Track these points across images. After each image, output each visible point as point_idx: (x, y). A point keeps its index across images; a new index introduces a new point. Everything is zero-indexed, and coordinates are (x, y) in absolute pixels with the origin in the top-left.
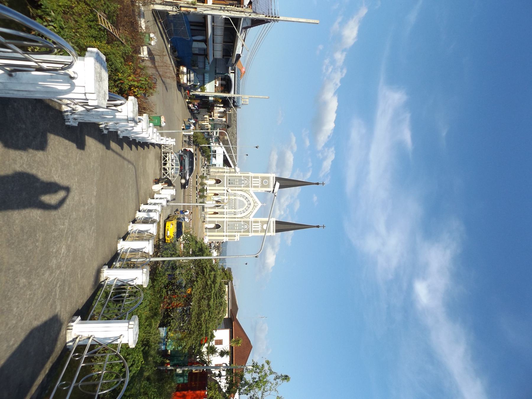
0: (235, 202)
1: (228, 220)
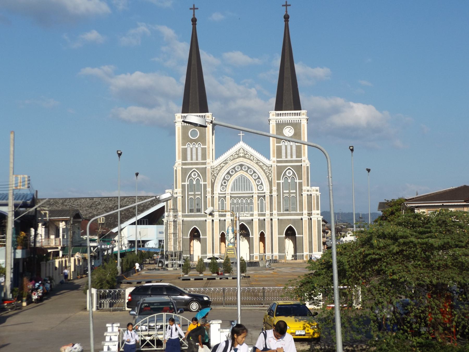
0: (237, 197)
1: (275, 212)
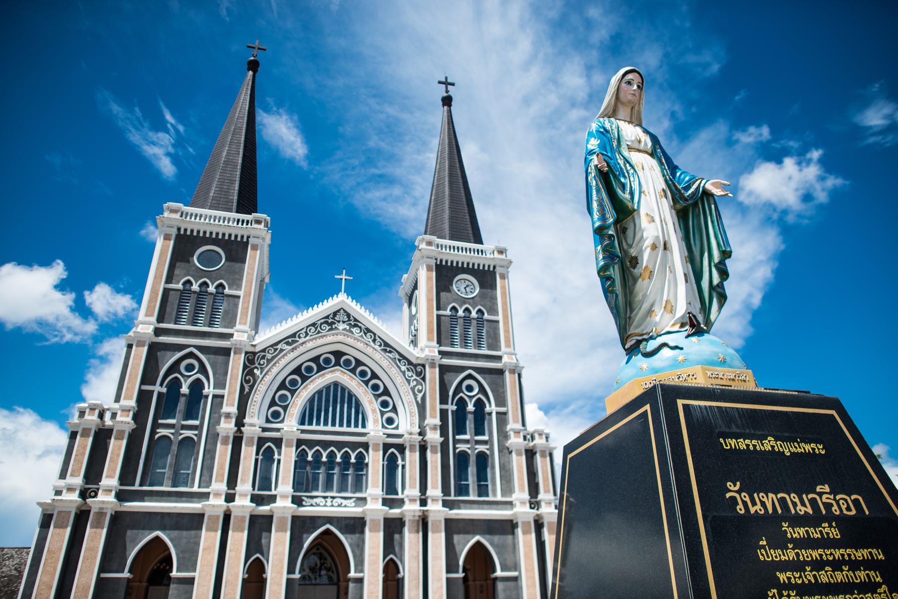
0: (318, 443)
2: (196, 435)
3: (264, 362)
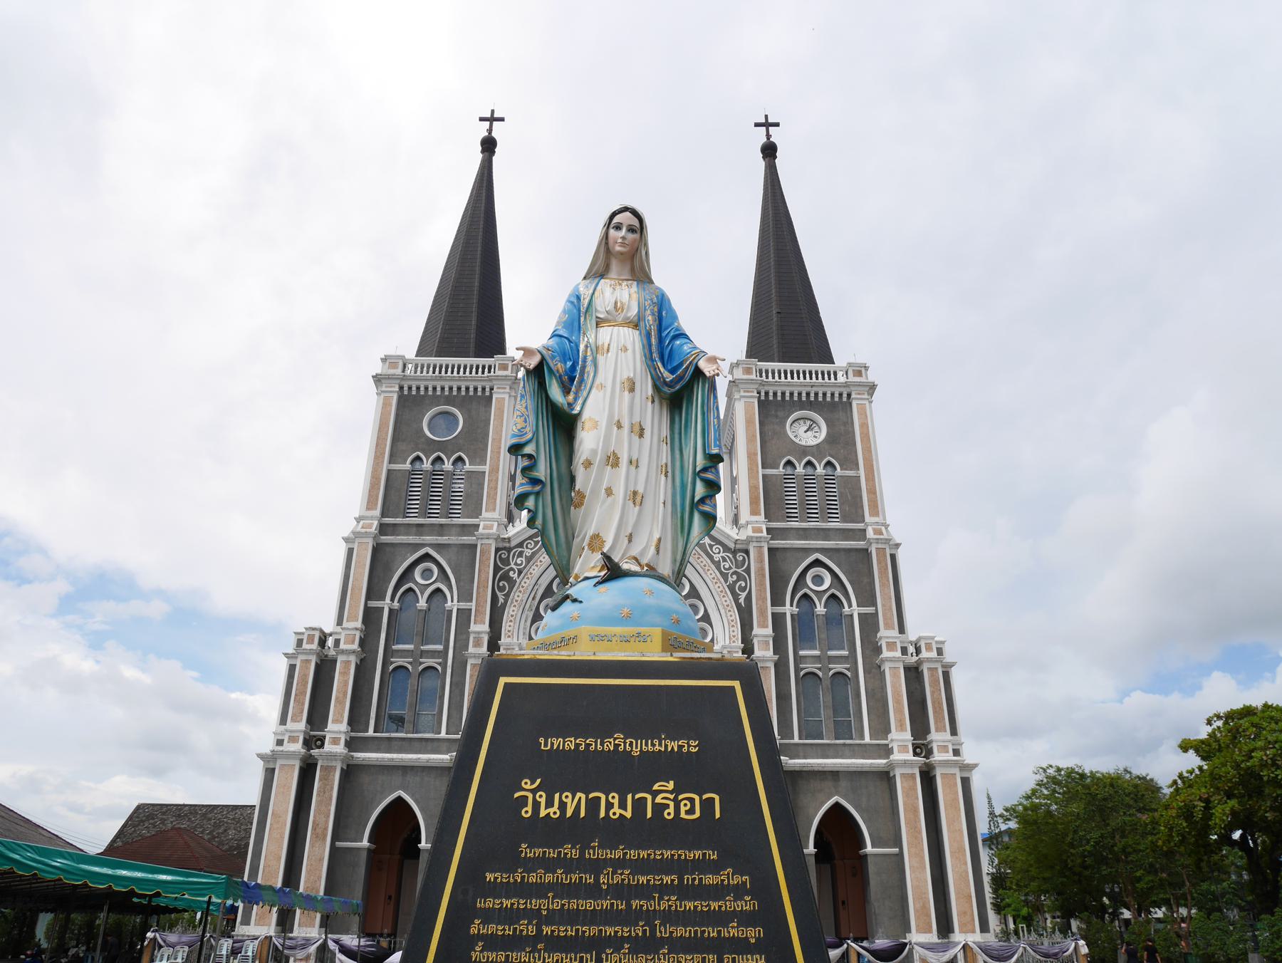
2: (439, 664)
3: (522, 561)
